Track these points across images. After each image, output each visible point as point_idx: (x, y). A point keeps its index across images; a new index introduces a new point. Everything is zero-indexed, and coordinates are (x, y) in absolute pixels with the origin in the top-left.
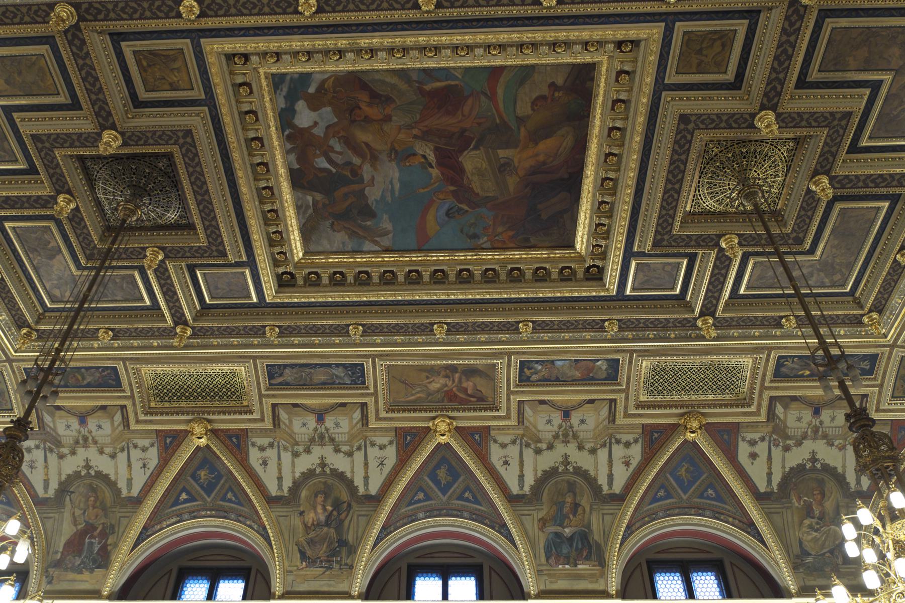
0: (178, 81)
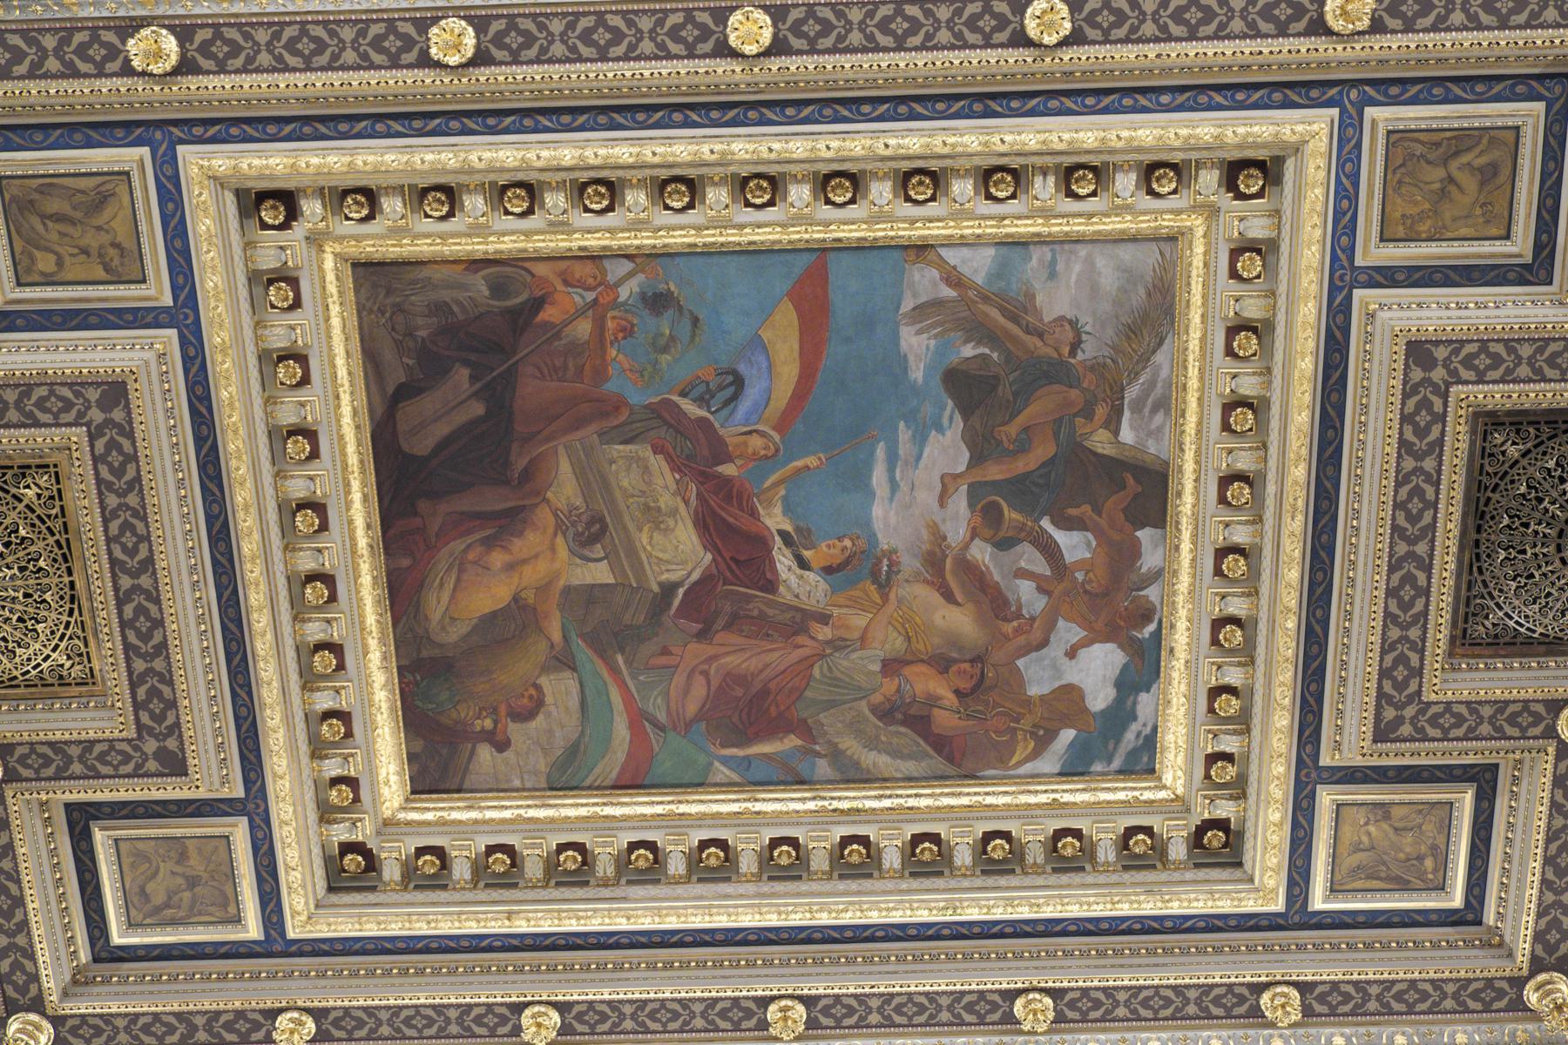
0: (1366, 824)
